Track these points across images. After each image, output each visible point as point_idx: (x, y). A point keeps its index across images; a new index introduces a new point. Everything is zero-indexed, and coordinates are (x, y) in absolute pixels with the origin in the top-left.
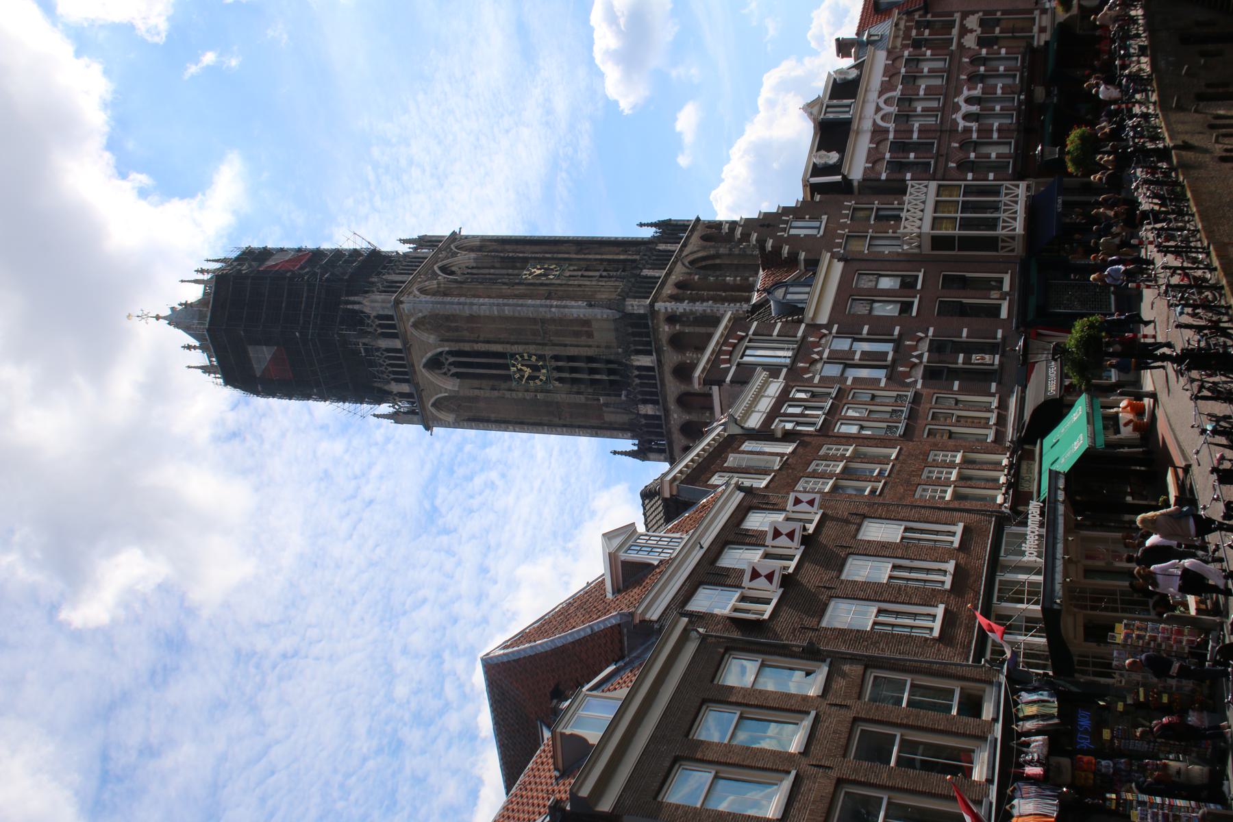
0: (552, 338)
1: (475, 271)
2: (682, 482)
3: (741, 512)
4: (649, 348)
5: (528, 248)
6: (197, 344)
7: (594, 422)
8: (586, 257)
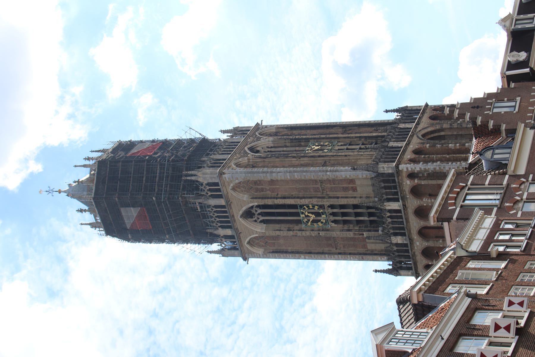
0: (328, 193)
1: (273, 149)
2: (425, 292)
3: (470, 312)
4: (396, 197)
5: (308, 131)
6: (86, 208)
7: (361, 250)
8: (349, 135)
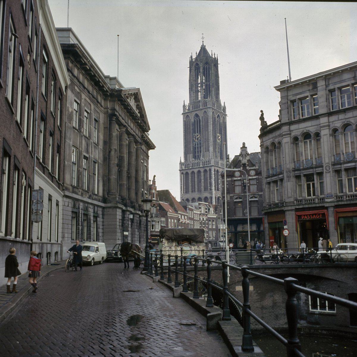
3: (186, 216)
